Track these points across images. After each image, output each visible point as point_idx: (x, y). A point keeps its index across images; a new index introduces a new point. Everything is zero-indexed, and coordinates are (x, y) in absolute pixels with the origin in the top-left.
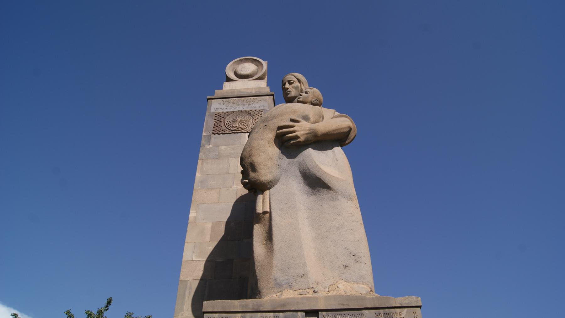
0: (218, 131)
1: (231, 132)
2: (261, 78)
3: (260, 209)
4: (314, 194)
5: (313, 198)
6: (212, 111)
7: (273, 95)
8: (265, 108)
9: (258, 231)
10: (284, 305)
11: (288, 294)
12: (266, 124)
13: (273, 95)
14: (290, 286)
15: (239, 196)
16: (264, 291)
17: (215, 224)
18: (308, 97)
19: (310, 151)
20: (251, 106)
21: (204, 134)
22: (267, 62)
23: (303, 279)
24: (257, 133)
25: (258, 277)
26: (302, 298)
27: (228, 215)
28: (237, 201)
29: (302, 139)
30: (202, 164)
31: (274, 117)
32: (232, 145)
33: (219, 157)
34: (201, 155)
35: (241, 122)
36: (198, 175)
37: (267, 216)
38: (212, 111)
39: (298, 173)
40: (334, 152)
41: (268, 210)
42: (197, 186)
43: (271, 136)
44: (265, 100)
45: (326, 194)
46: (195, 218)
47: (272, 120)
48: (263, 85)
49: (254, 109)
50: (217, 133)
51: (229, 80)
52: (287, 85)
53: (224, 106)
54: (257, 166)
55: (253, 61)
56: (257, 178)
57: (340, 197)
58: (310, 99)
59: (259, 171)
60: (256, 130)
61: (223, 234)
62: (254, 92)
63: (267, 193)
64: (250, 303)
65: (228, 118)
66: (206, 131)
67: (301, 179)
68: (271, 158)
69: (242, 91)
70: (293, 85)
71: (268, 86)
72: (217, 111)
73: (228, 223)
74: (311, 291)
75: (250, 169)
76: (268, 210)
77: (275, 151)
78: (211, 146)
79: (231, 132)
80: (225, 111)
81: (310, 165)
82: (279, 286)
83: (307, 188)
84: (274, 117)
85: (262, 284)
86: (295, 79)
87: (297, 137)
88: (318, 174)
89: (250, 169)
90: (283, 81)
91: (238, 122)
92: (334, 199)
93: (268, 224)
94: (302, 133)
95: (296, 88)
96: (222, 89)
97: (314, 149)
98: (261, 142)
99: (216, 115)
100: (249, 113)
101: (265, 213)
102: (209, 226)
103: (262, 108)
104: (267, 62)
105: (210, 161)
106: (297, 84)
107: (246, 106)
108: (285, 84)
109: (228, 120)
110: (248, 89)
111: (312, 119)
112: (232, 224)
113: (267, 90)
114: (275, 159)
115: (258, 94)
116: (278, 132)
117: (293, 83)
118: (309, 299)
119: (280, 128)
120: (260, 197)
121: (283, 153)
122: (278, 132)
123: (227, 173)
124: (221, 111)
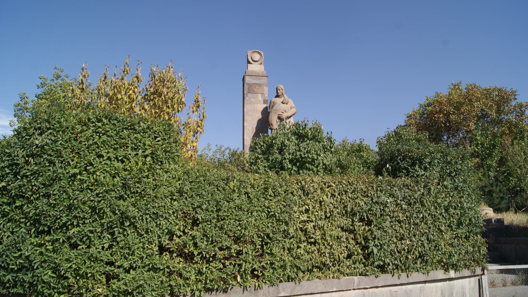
2: (261, 64)
17: (252, 128)
31: (277, 110)
33: (251, 103)
35: (257, 89)
38: (247, 82)
43: (277, 116)
49: (261, 83)
52: (279, 91)
62: (260, 74)
73: (256, 128)
80: (252, 82)
90: (277, 88)
102: (250, 128)
111: (287, 111)
115: (262, 75)
124: (250, 82)
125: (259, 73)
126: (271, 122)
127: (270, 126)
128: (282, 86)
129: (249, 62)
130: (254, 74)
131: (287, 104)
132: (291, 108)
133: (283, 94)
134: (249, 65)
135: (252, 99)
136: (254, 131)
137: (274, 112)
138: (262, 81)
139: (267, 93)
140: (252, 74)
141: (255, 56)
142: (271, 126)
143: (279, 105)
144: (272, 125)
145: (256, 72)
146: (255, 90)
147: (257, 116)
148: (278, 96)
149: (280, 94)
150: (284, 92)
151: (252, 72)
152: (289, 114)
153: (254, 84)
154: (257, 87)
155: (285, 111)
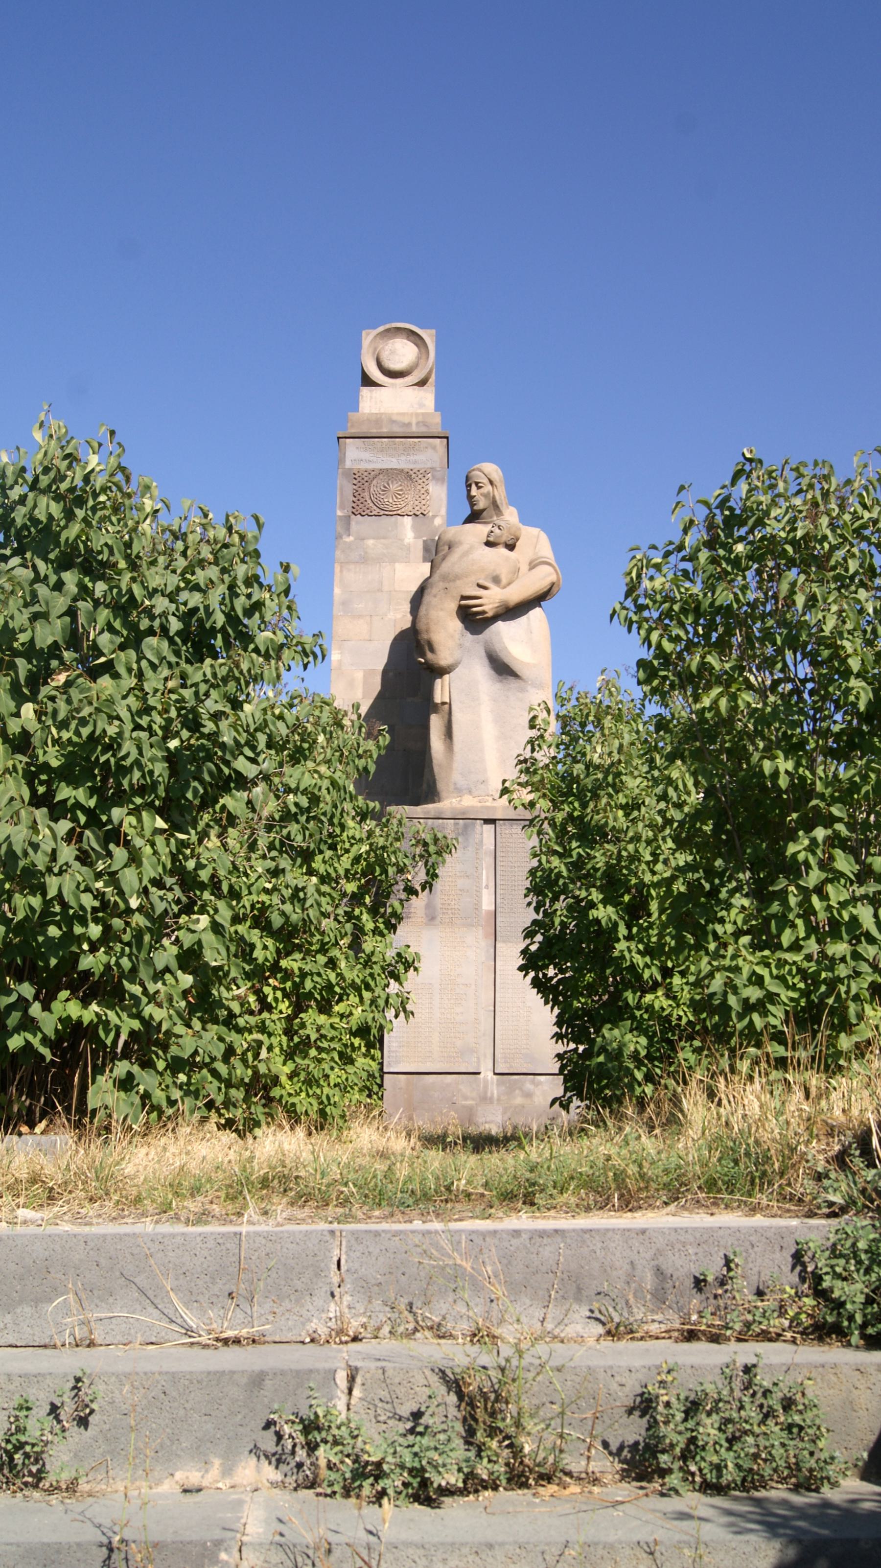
0: (359, 509)
1: (382, 512)
2: (422, 383)
3: (438, 699)
5: (498, 686)
6: (348, 464)
7: (447, 438)
8: (434, 465)
9: (436, 722)
10: (464, 813)
11: (468, 802)
12: (447, 585)
13: (447, 438)
14: (470, 792)
15: (398, 631)
16: (443, 794)
17: (368, 674)
18: (501, 536)
19: (500, 625)
20: (412, 458)
21: (339, 513)
22: (434, 331)
23: (482, 786)
24: (435, 596)
26: (482, 807)
27: (384, 660)
28: (395, 639)
29: (490, 614)
30: (341, 571)
31: (457, 577)
32: (384, 538)
33: (365, 560)
34: (338, 554)
35: (397, 494)
36: (337, 591)
37: (446, 706)
38: (348, 464)
39: (483, 654)
40: (528, 618)
42: (337, 610)
43: (453, 606)
44: (434, 448)
45: (512, 683)
46: (340, 661)
47: (454, 581)
48: (427, 398)
49: (416, 467)
51: (367, 381)
52: (474, 491)
53: (365, 455)
54: (436, 646)
55: (413, 336)
56: (435, 661)
57: (529, 688)
58: (504, 539)
59: (438, 653)
60: (434, 591)
62: (414, 429)
63: (446, 677)
64: (430, 808)
65: (374, 482)
66: (342, 508)
67: (486, 661)
68: (452, 637)
69: (395, 418)
70: (482, 490)
71: (436, 410)
72: (356, 466)
73: (385, 673)
74: (490, 799)
75: (427, 648)
76: (447, 700)
77: (456, 625)
78: (351, 538)
79: (382, 512)
80: (370, 466)
81: (497, 647)
82: (459, 791)
83: (493, 672)
84: (457, 577)
85: (441, 786)
86: (486, 481)
87: (484, 612)
88: (506, 660)
89: (427, 648)
90: (467, 478)
91: (390, 494)
92: (522, 690)
93: (446, 716)
94: (491, 606)
95: (486, 496)
96: (357, 411)
97: (504, 620)
98: (441, 614)
100: (408, 476)
101: (443, 703)
102: (359, 675)
103: (429, 465)
104: (434, 331)
105: (352, 567)
106: (488, 488)
107: (403, 458)
108: (470, 486)
109: (376, 487)
110: (403, 414)
111: (504, 581)
112: (391, 674)
113: (436, 423)
114: (457, 636)
115: (423, 430)
116: (463, 602)
117: (481, 487)
118: (488, 808)
119: (464, 598)
120: (438, 682)
121: (467, 628)
122: (463, 602)
123: (380, 590)
125: (409, 425)
126: (425, 636)
127: (423, 655)
128: (491, 469)
129: (367, 381)
130: (385, 430)
131: (511, 547)
132: (532, 566)
133: (495, 505)
134: (366, 392)
135: (370, 542)
136: (376, 686)
137: (441, 585)
139: (443, 511)
140: (374, 431)
141: (393, 352)
142: (429, 655)
143: (472, 548)
144: (432, 650)
145: (393, 422)
146: (389, 499)
147: (391, 616)
148: (474, 517)
149: (481, 504)
150: (500, 494)
151: (378, 420)
152: (515, 594)
153: (381, 471)
154: (394, 487)
155: (496, 580)
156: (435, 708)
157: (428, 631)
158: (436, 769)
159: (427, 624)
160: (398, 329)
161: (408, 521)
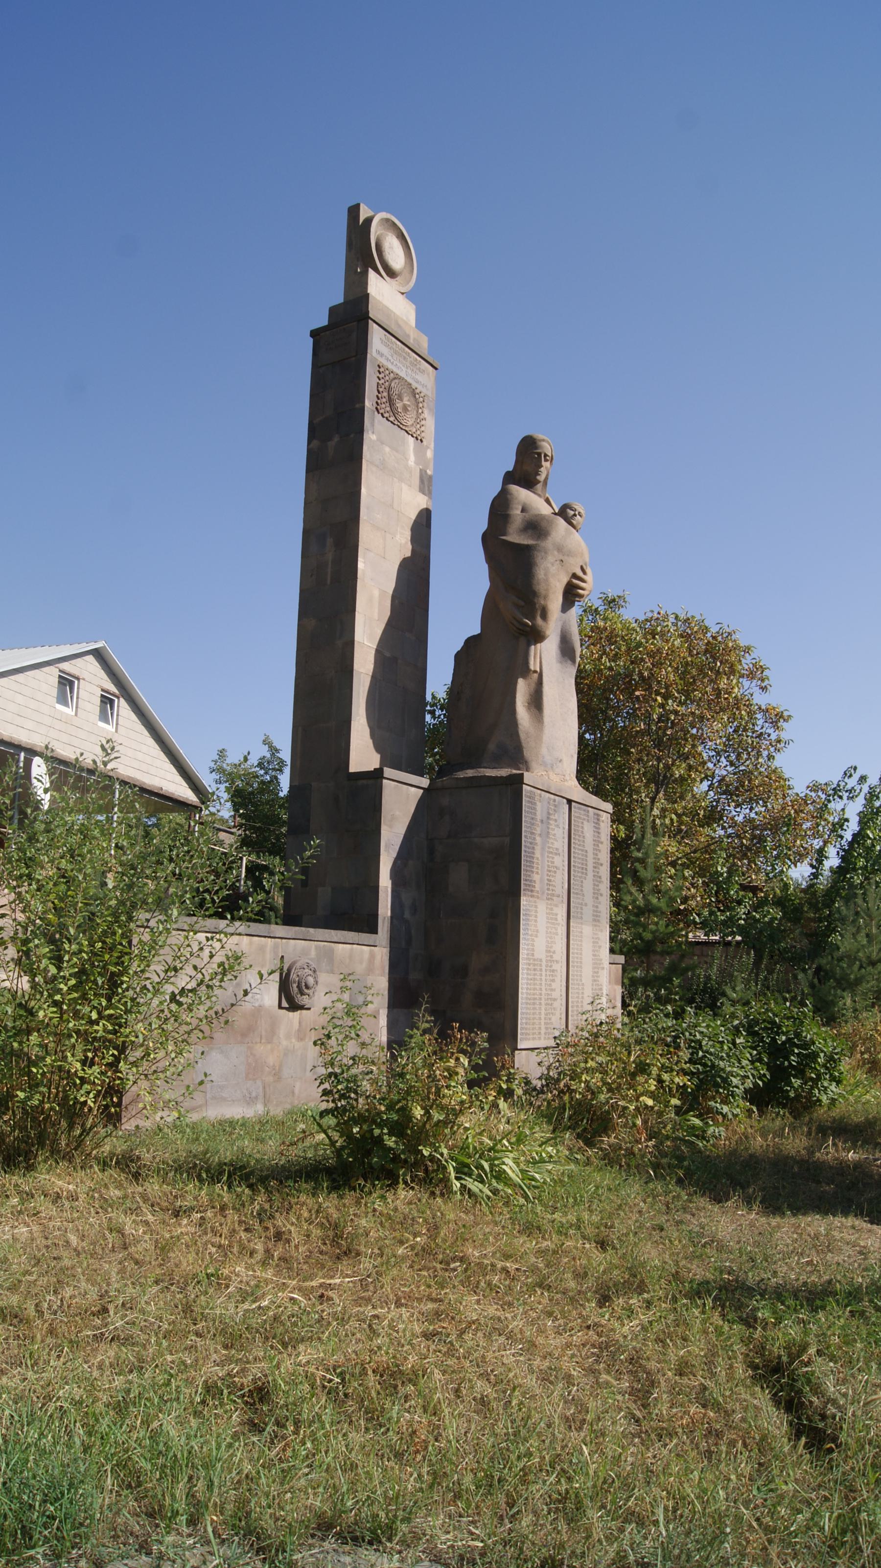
4: (561, 662)
5: (559, 665)
9: (522, 689)
23: (560, 764)
25: (524, 745)
32: (397, 451)
41: (538, 670)
50: (382, 415)
61: (389, 614)
69: (401, 323)
73: (394, 597)
75: (539, 613)
76: (538, 670)
79: (396, 422)
83: (559, 652)
89: (539, 613)
99: (379, 366)
101: (535, 672)
102: (376, 593)
120: (533, 647)
127: (532, 618)
138: (419, 377)
145: (399, 326)
156: (525, 671)
157: (546, 597)
158: (522, 736)
159: (547, 590)
160: (394, 224)
161: (411, 440)
